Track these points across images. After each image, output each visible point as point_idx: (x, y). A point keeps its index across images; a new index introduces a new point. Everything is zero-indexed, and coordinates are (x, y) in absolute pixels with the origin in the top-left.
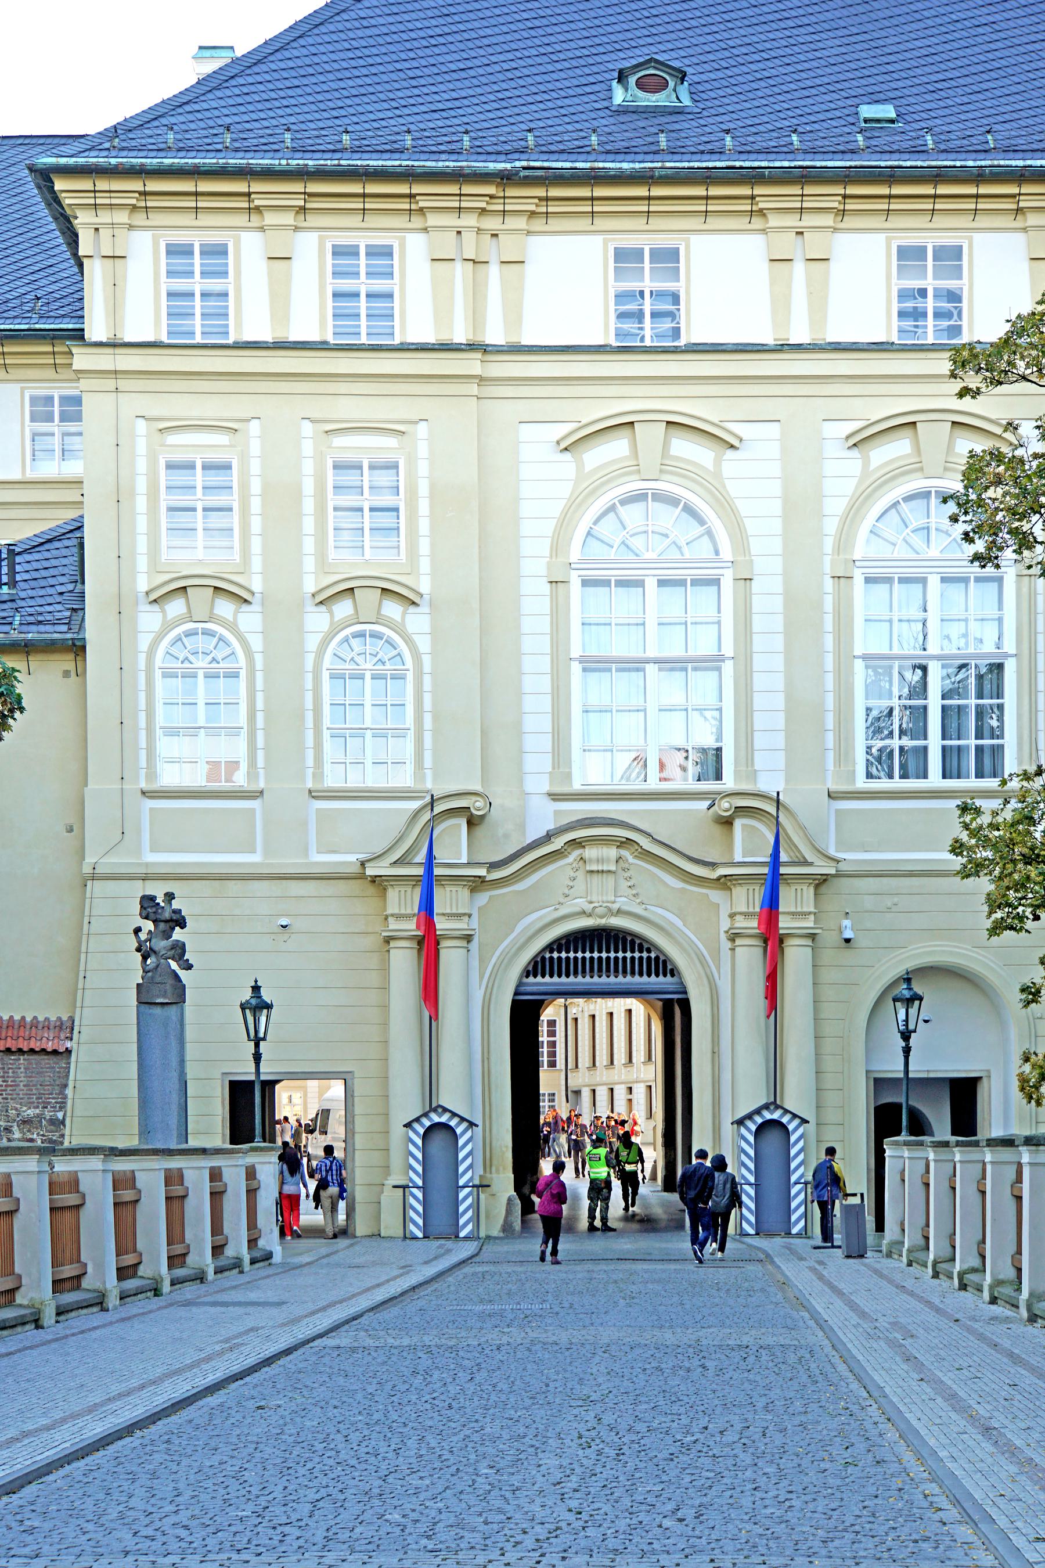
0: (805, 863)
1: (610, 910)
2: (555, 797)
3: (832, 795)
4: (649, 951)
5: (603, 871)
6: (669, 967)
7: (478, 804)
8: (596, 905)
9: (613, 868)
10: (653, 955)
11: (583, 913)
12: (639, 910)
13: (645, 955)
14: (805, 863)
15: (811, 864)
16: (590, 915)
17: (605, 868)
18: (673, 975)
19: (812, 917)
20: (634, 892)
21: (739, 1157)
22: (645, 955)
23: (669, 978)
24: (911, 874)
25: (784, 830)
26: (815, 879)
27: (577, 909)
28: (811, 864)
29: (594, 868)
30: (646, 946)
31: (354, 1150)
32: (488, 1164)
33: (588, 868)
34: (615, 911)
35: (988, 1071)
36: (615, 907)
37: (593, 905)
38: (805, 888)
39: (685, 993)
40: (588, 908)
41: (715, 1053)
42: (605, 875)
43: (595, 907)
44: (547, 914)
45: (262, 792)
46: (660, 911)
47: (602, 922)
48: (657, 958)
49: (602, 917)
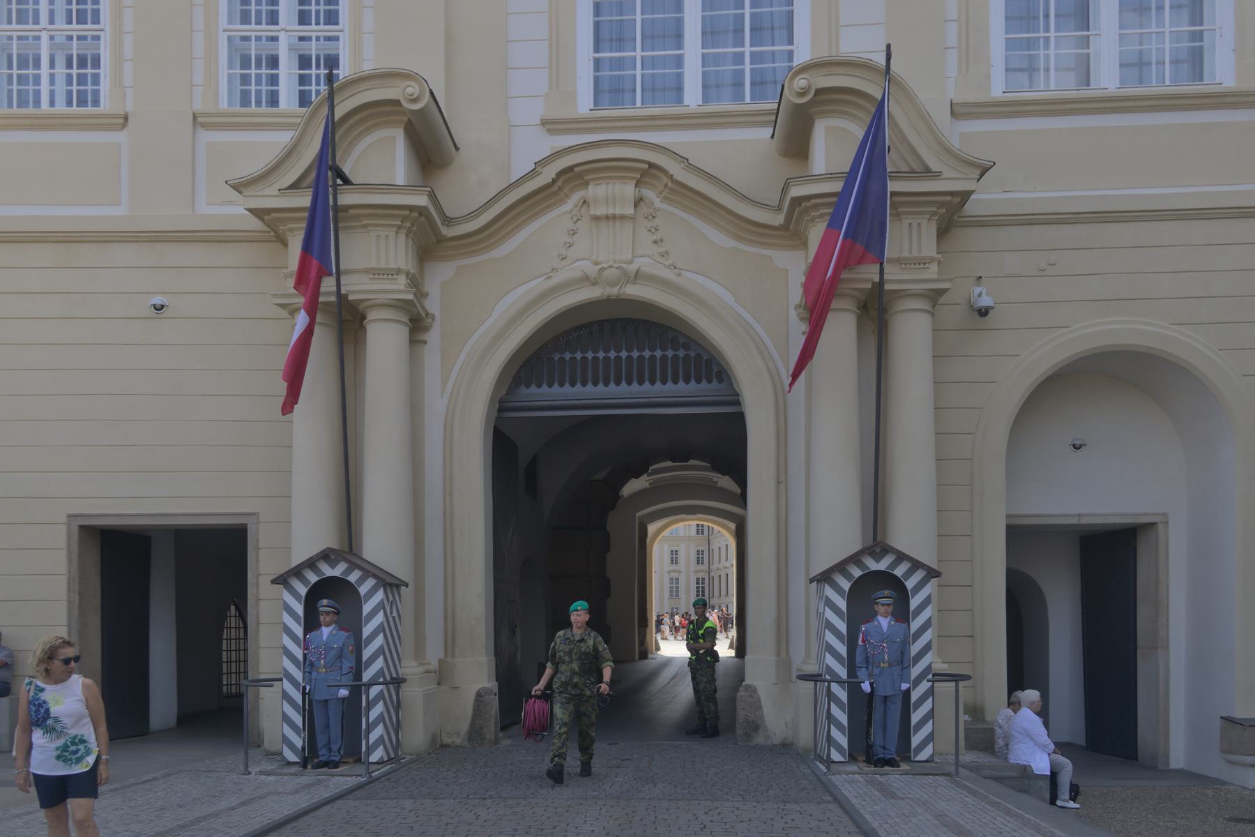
0: (927, 173)
1: (625, 273)
2: (552, 126)
3: (956, 109)
4: (686, 347)
5: (614, 217)
6: (715, 369)
7: (410, 90)
8: (605, 265)
9: (630, 211)
10: (692, 354)
11: (586, 280)
12: (669, 275)
13: (681, 353)
14: (927, 173)
15: (937, 175)
16: (595, 283)
17: (618, 211)
18: (720, 380)
19: (934, 268)
20: (662, 250)
21: (821, 636)
22: (681, 353)
23: (715, 384)
24: (1076, 218)
25: (895, 124)
26: (942, 204)
27: (578, 274)
28: (937, 175)
29: (601, 211)
30: (682, 341)
31: (258, 623)
32: (450, 644)
33: (592, 212)
34: (633, 274)
35: (1165, 514)
36: (633, 267)
37: (600, 266)
38: (924, 223)
39: (738, 403)
40: (592, 270)
41: (781, 481)
42: (618, 224)
43: (602, 269)
44: (538, 285)
45: (126, 118)
46: (700, 279)
47: (615, 291)
48: (699, 356)
49: (613, 284)
